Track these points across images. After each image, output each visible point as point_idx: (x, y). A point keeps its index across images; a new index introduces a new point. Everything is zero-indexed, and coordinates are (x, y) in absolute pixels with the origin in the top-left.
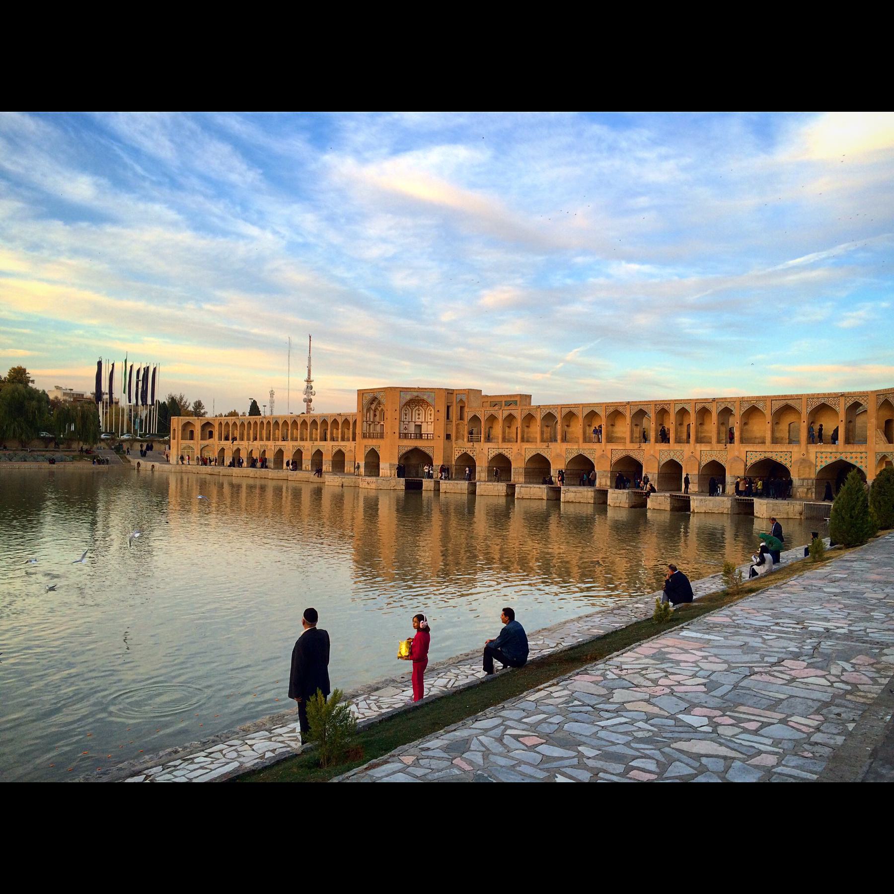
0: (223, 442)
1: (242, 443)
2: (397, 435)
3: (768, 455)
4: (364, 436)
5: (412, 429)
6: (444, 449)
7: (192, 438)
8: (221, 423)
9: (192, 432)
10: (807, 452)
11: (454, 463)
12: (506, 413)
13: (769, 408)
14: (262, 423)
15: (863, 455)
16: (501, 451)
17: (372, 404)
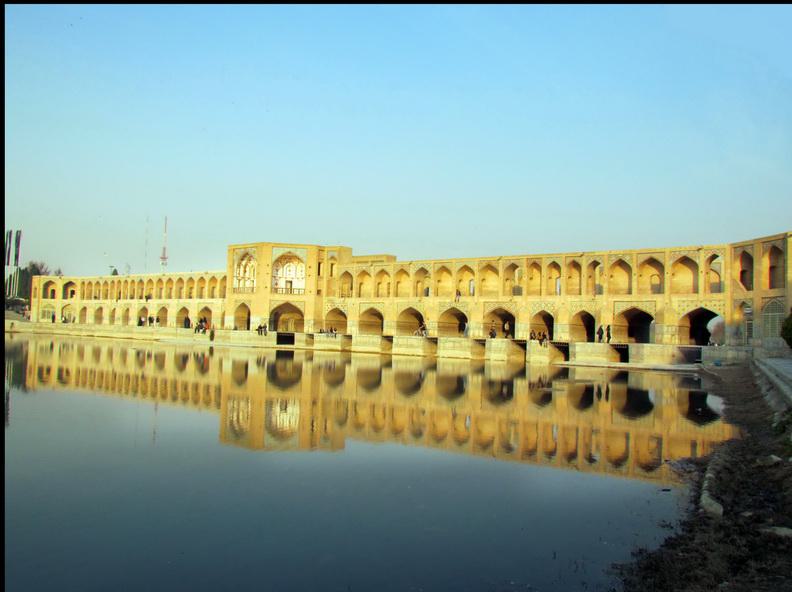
0: (85, 301)
1: (105, 301)
2: (269, 289)
3: (635, 305)
4: (235, 290)
5: (282, 284)
6: (316, 303)
7: (53, 297)
8: (83, 283)
9: (53, 291)
10: (670, 301)
11: (324, 318)
12: (378, 269)
13: (635, 261)
14: (119, 282)
15: (722, 303)
16: (372, 306)
17: (242, 260)
